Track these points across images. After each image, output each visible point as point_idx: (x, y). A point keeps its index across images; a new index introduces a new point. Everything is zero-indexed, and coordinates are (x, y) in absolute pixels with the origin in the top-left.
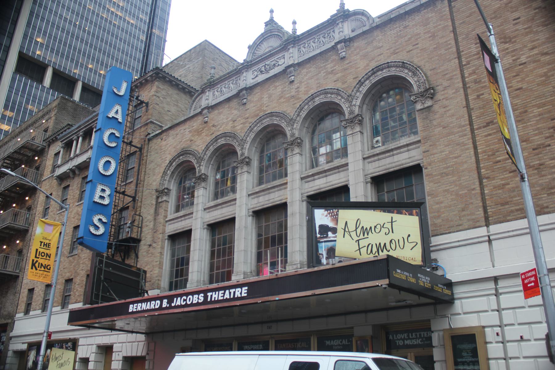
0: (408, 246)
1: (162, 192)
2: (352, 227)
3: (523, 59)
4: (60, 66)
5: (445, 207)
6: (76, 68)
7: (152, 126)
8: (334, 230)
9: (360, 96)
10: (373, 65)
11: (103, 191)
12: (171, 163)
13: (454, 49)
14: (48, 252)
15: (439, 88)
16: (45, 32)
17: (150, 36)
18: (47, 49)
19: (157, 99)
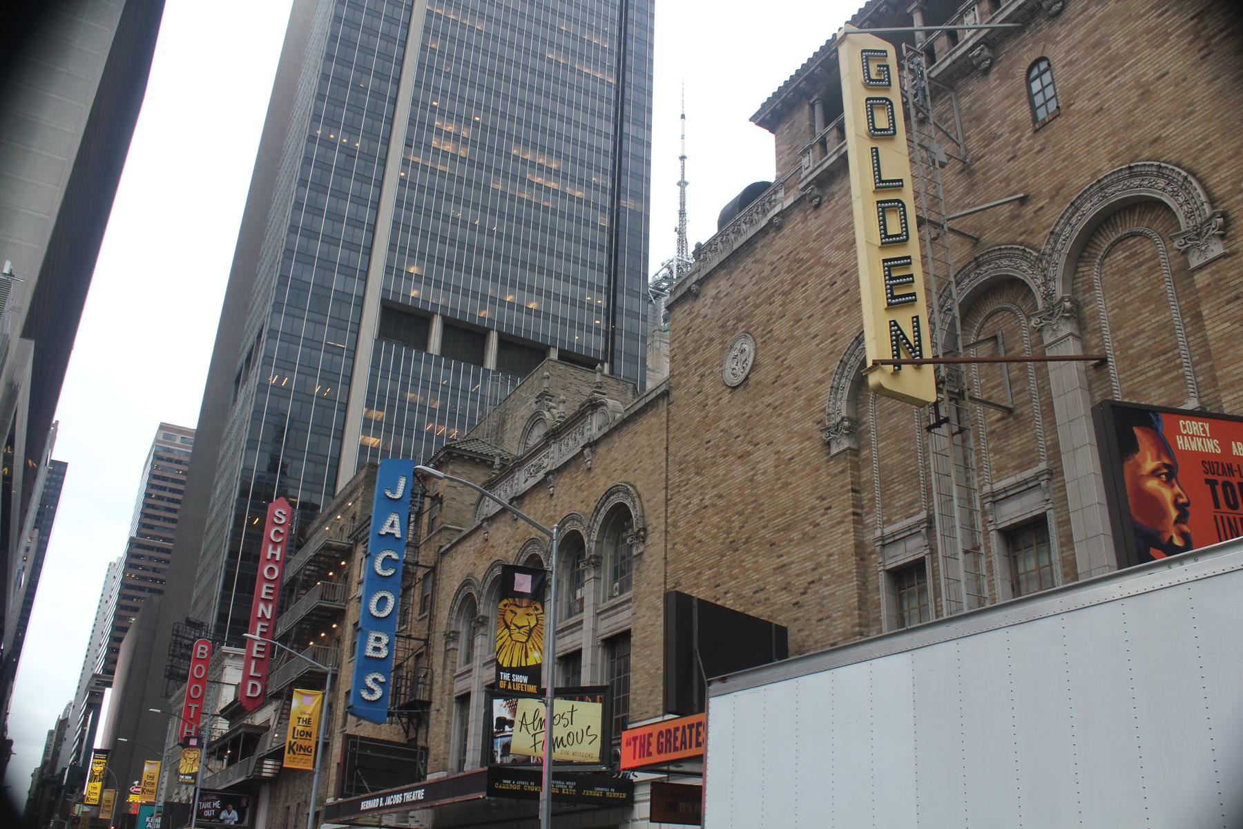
0: (587, 739)
1: (452, 636)
2: (529, 719)
3: (707, 502)
4: (454, 310)
5: (642, 688)
6: (483, 308)
7: (446, 534)
8: (511, 723)
9: (597, 527)
10: (610, 484)
11: (378, 639)
12: (457, 595)
13: (663, 476)
14: (308, 729)
15: (650, 528)
16: (422, 254)
17: (616, 214)
18: (428, 284)
19: (453, 491)
